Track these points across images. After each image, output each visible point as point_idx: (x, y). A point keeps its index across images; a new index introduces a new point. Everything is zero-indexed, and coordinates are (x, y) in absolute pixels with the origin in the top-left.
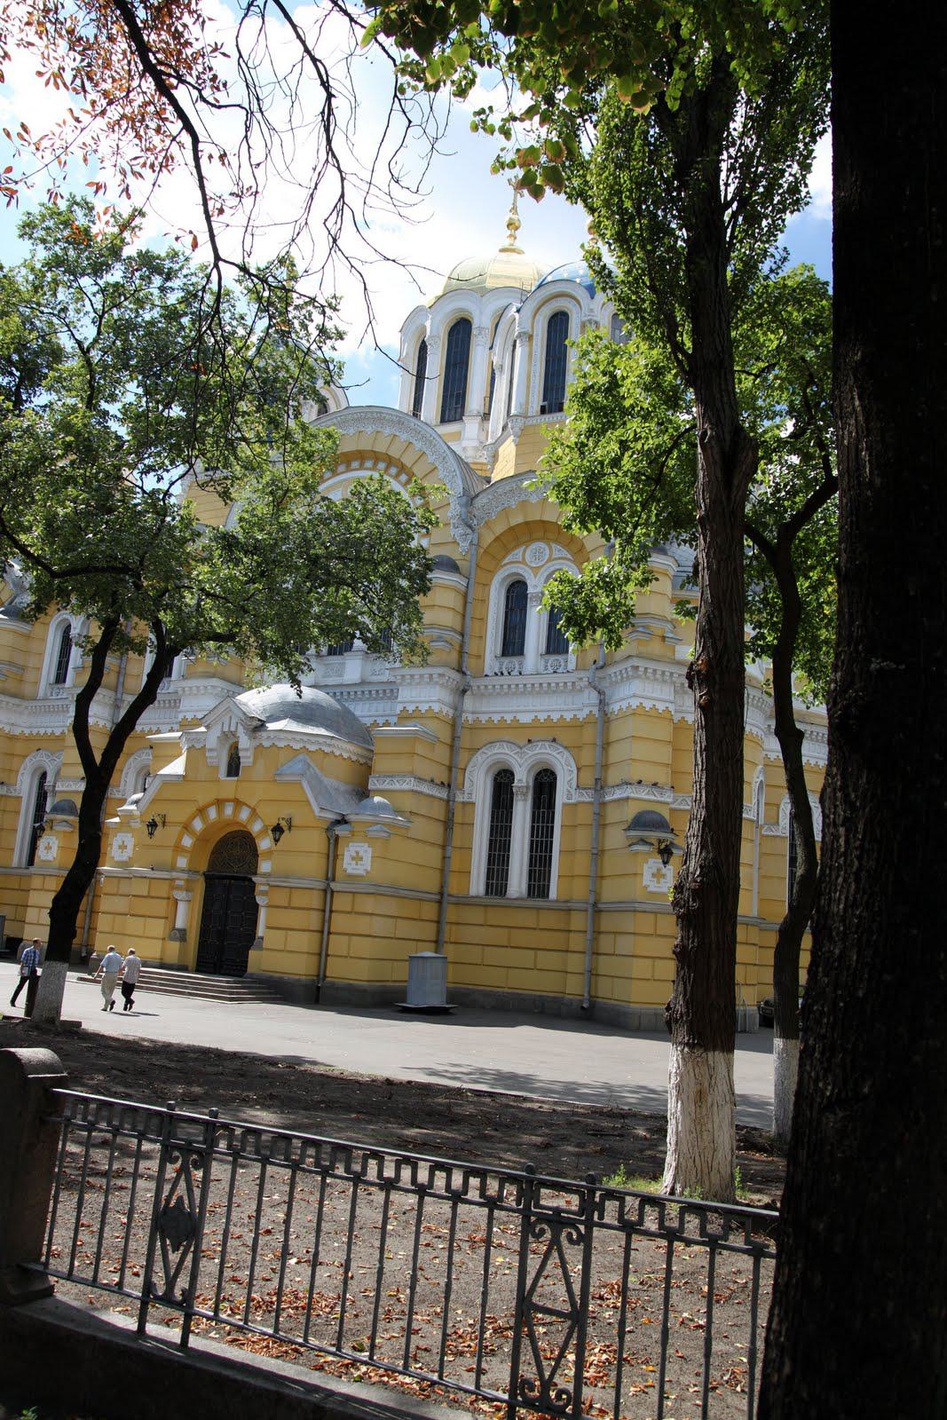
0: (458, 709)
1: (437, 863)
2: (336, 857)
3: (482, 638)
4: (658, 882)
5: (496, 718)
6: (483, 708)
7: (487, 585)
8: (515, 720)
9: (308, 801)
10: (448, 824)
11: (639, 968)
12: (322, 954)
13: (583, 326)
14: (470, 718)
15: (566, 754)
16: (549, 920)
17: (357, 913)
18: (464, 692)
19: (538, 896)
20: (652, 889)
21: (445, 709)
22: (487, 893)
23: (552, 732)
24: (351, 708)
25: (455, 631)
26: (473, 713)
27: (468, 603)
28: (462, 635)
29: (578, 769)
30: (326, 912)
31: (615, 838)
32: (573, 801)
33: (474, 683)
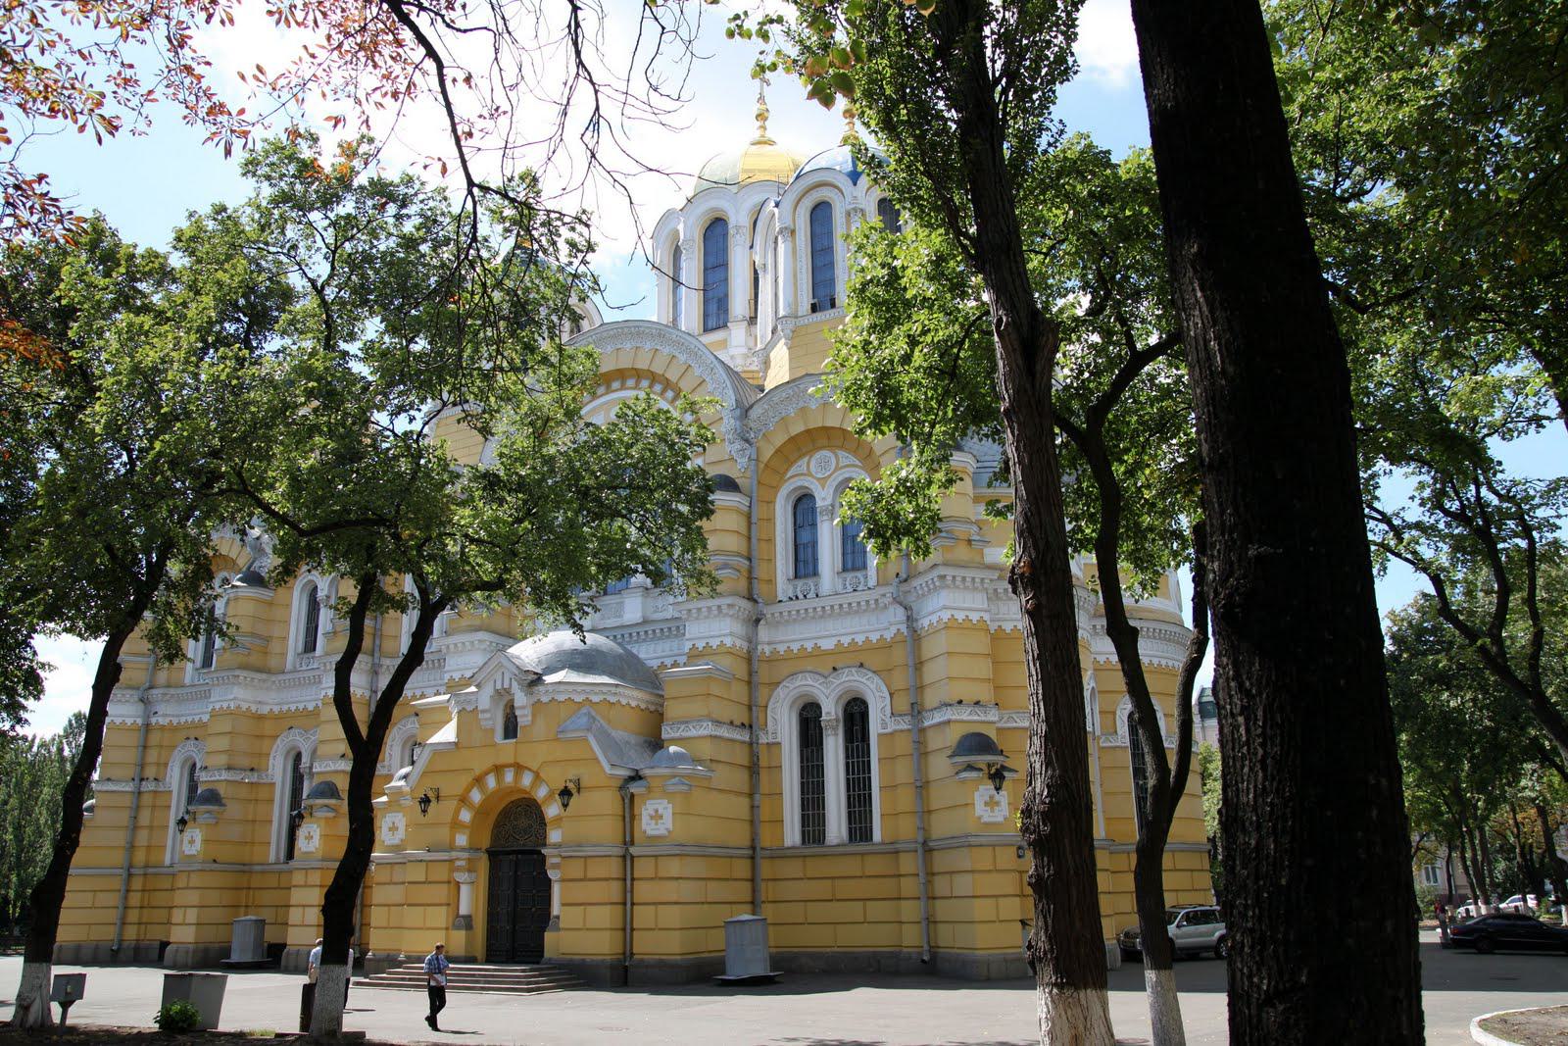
0: (752, 640)
1: (745, 813)
2: (633, 817)
3: (771, 560)
4: (992, 811)
5: (795, 647)
6: (781, 638)
7: (771, 502)
8: (817, 647)
9: (596, 759)
10: (753, 769)
11: (982, 909)
12: (627, 929)
13: (848, 214)
14: (767, 649)
15: (876, 679)
16: (875, 865)
17: (661, 879)
18: (758, 621)
19: (861, 840)
20: (986, 819)
21: (738, 643)
22: (804, 842)
23: (858, 656)
24: (635, 651)
25: (741, 556)
26: (769, 643)
27: (753, 525)
28: (750, 560)
29: (891, 695)
30: (627, 880)
31: (940, 766)
32: (889, 730)
33: (768, 611)
